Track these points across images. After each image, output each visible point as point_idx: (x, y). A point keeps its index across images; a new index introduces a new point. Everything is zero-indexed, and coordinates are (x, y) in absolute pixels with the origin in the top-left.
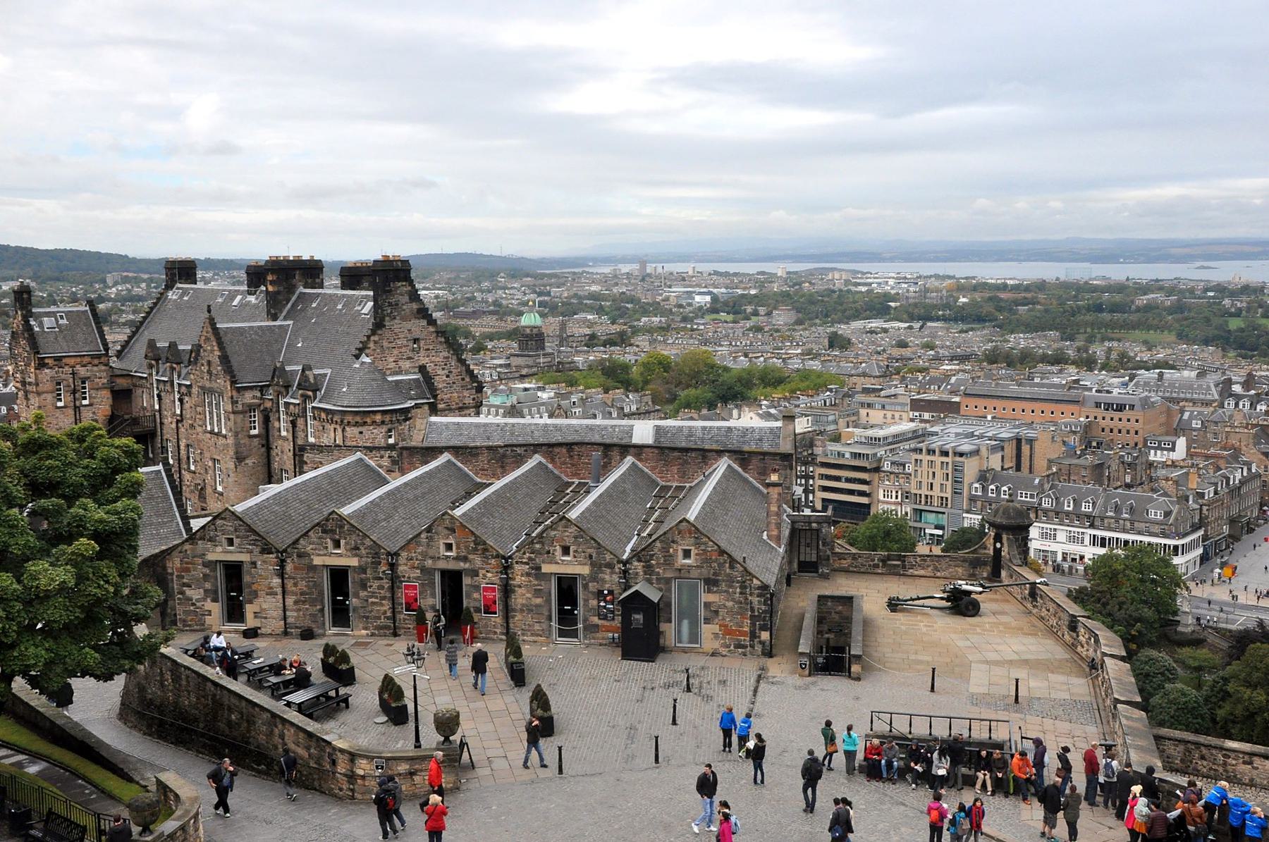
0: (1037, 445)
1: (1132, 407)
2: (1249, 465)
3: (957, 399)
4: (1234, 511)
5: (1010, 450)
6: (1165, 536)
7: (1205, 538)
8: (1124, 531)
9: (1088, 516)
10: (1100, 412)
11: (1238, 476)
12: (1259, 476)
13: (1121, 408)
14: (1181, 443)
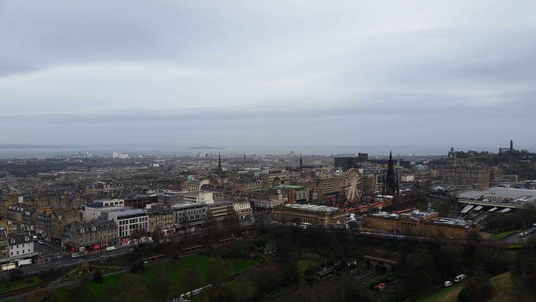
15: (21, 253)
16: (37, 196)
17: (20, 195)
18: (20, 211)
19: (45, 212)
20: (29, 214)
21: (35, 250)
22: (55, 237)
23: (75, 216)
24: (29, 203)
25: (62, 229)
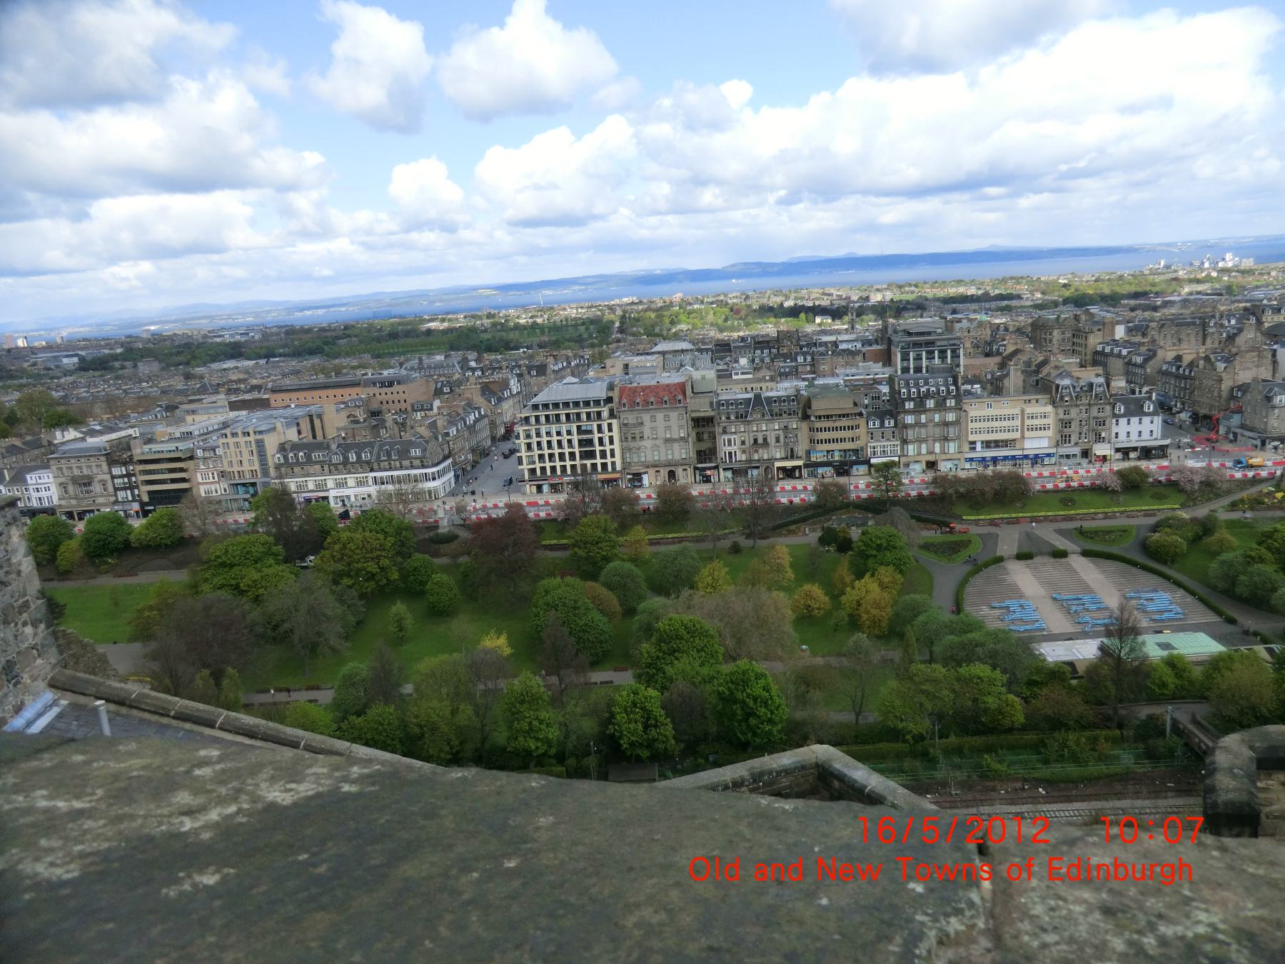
0: (325, 418)
1: (399, 383)
2: (478, 409)
3: (266, 396)
4: (473, 443)
5: (305, 426)
6: (423, 467)
7: (454, 463)
8: (396, 469)
9: (368, 463)
10: (376, 390)
11: (472, 417)
12: (486, 416)
13: (391, 384)
14: (437, 403)
15: (1134, 436)
16: (1153, 325)
17: (1118, 323)
18: (1119, 355)
19: (1179, 358)
20: (1139, 360)
21: (1164, 437)
22: (1203, 411)
23: (1258, 366)
24: (1138, 339)
25: (1225, 394)
